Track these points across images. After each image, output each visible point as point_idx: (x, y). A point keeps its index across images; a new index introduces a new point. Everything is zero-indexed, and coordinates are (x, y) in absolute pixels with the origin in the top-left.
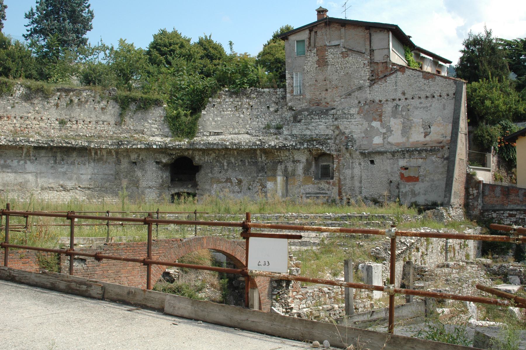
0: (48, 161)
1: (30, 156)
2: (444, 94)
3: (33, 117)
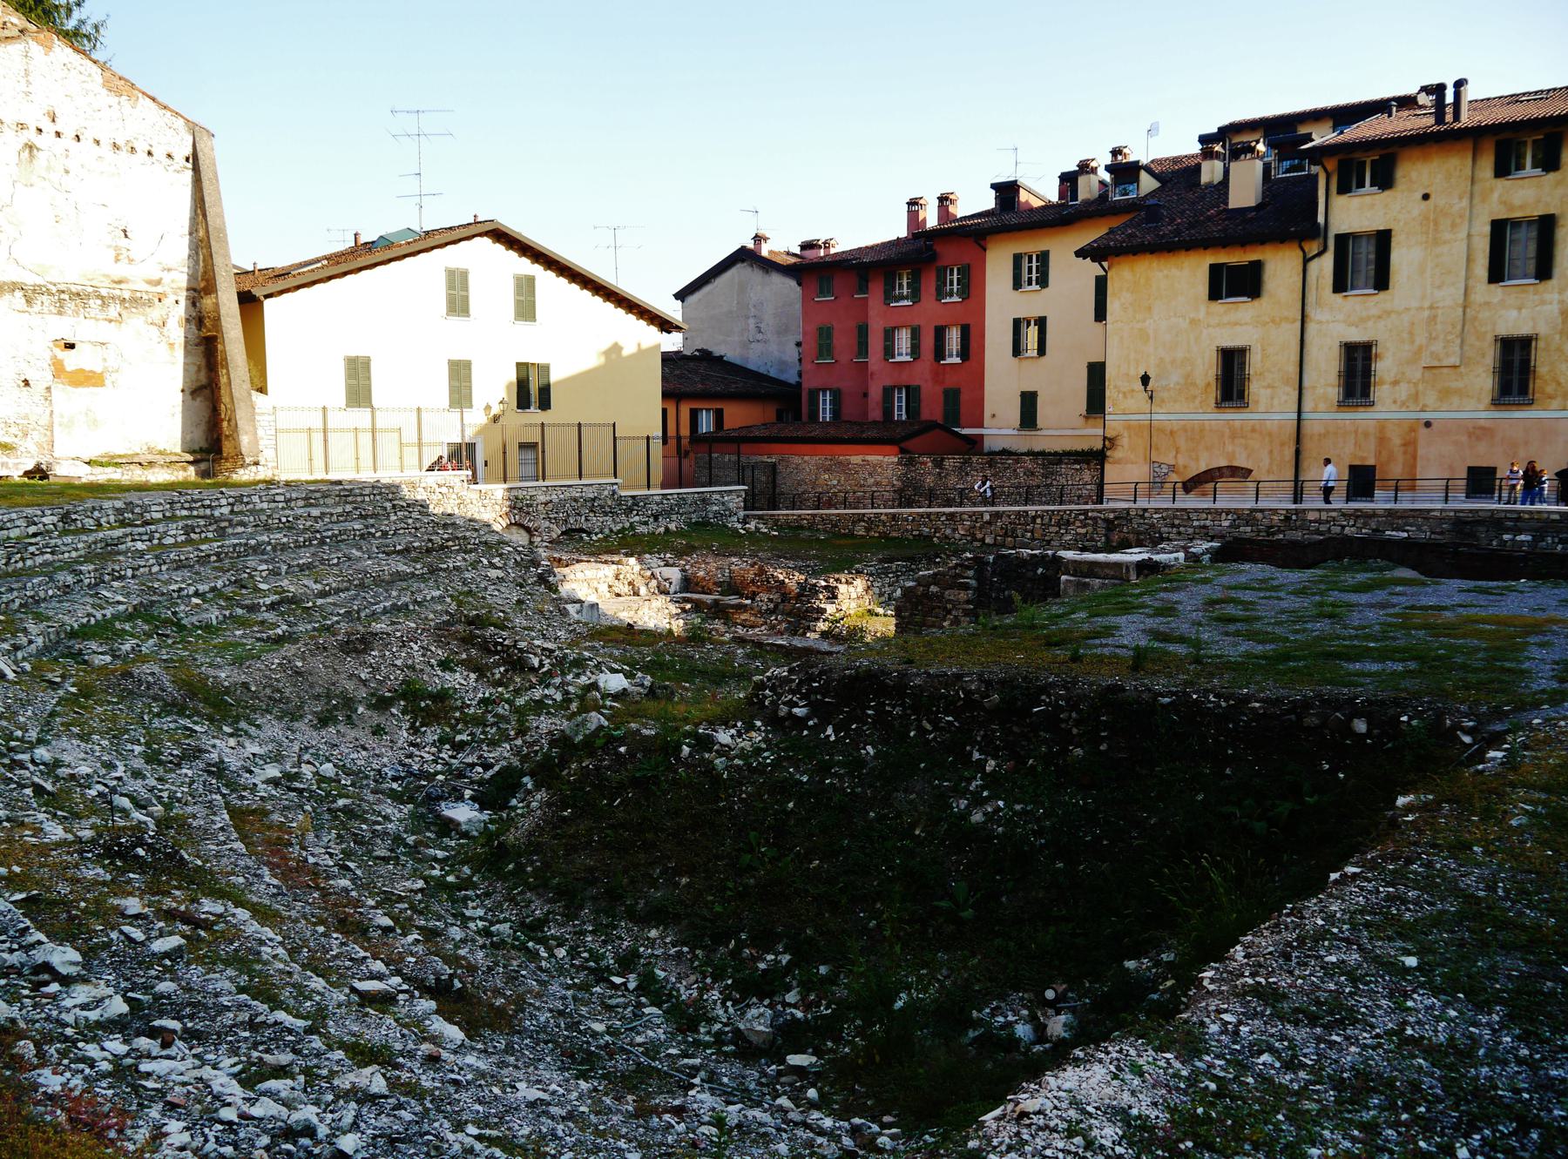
2: (159, 153)
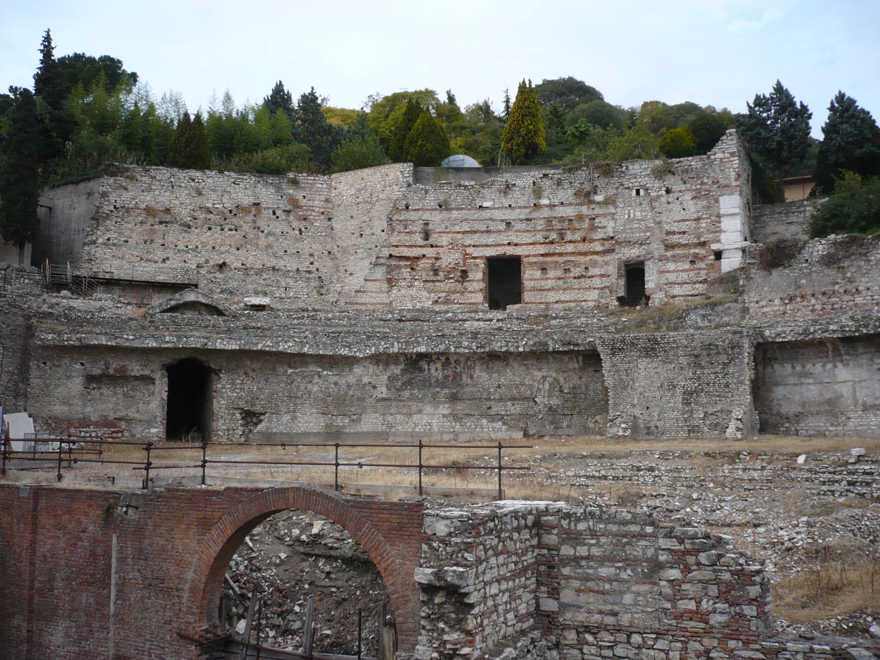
0: (872, 361)
1: (840, 355)
3: (842, 290)
